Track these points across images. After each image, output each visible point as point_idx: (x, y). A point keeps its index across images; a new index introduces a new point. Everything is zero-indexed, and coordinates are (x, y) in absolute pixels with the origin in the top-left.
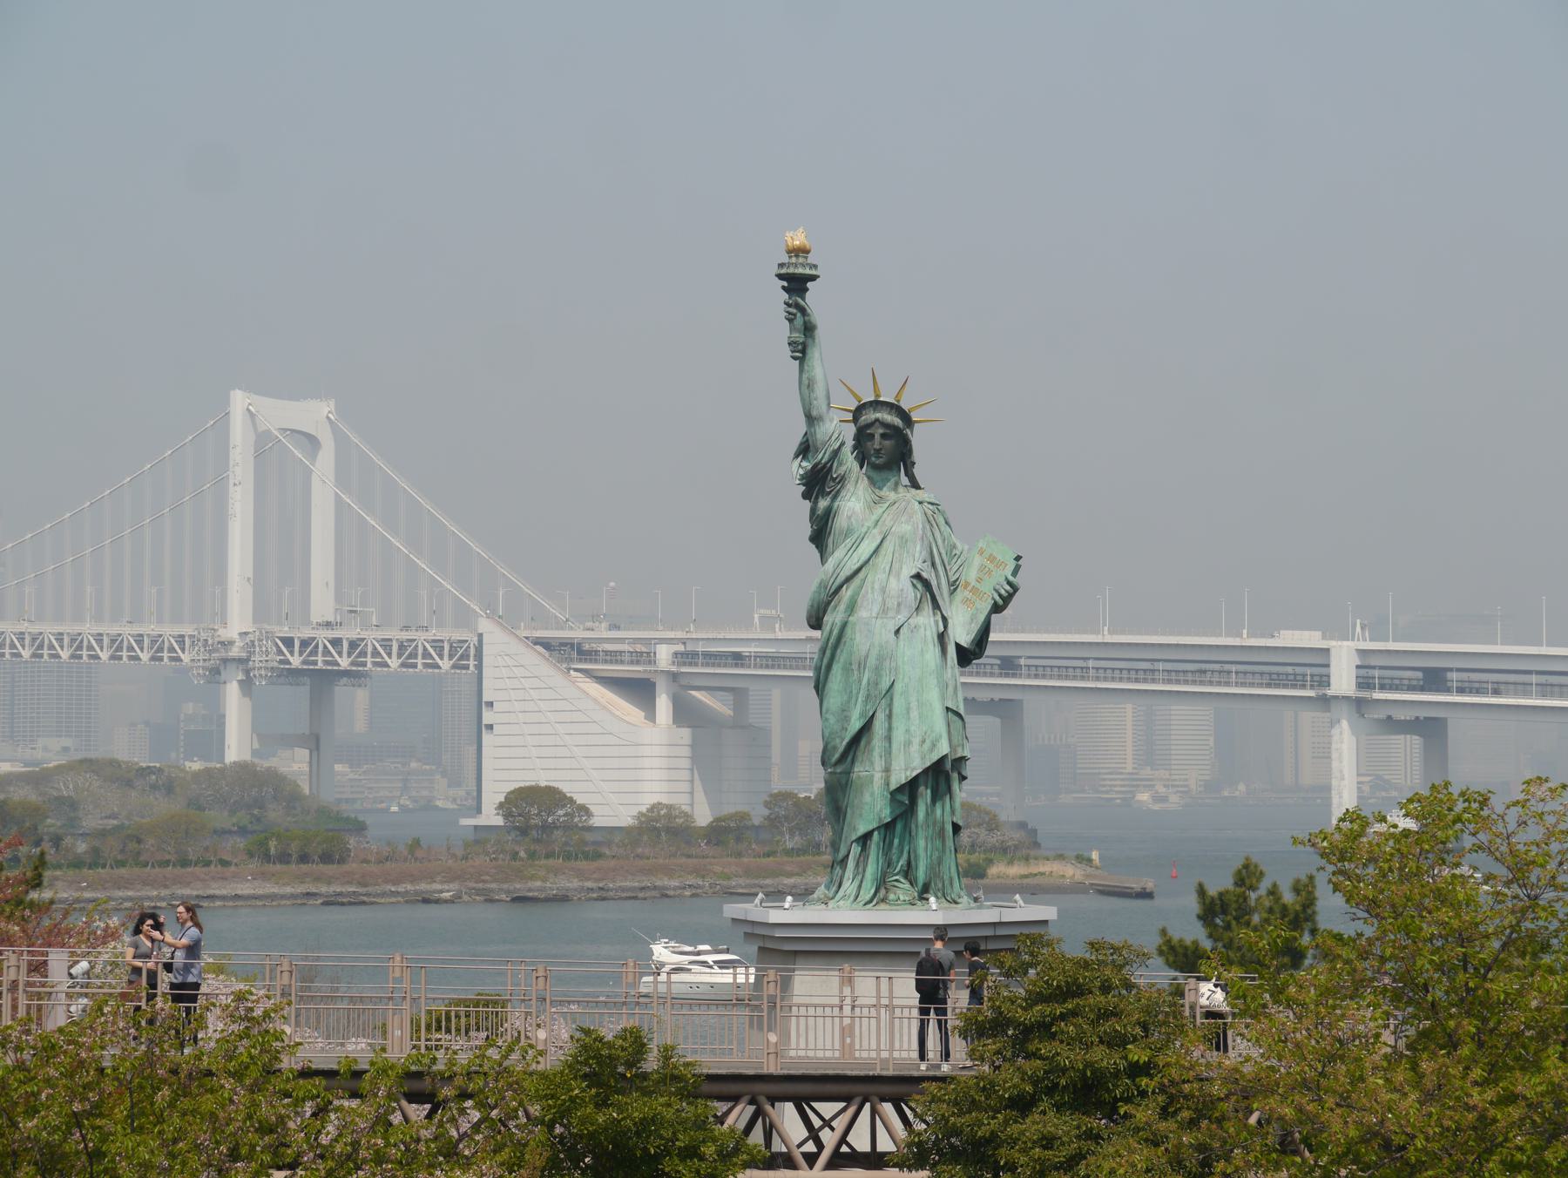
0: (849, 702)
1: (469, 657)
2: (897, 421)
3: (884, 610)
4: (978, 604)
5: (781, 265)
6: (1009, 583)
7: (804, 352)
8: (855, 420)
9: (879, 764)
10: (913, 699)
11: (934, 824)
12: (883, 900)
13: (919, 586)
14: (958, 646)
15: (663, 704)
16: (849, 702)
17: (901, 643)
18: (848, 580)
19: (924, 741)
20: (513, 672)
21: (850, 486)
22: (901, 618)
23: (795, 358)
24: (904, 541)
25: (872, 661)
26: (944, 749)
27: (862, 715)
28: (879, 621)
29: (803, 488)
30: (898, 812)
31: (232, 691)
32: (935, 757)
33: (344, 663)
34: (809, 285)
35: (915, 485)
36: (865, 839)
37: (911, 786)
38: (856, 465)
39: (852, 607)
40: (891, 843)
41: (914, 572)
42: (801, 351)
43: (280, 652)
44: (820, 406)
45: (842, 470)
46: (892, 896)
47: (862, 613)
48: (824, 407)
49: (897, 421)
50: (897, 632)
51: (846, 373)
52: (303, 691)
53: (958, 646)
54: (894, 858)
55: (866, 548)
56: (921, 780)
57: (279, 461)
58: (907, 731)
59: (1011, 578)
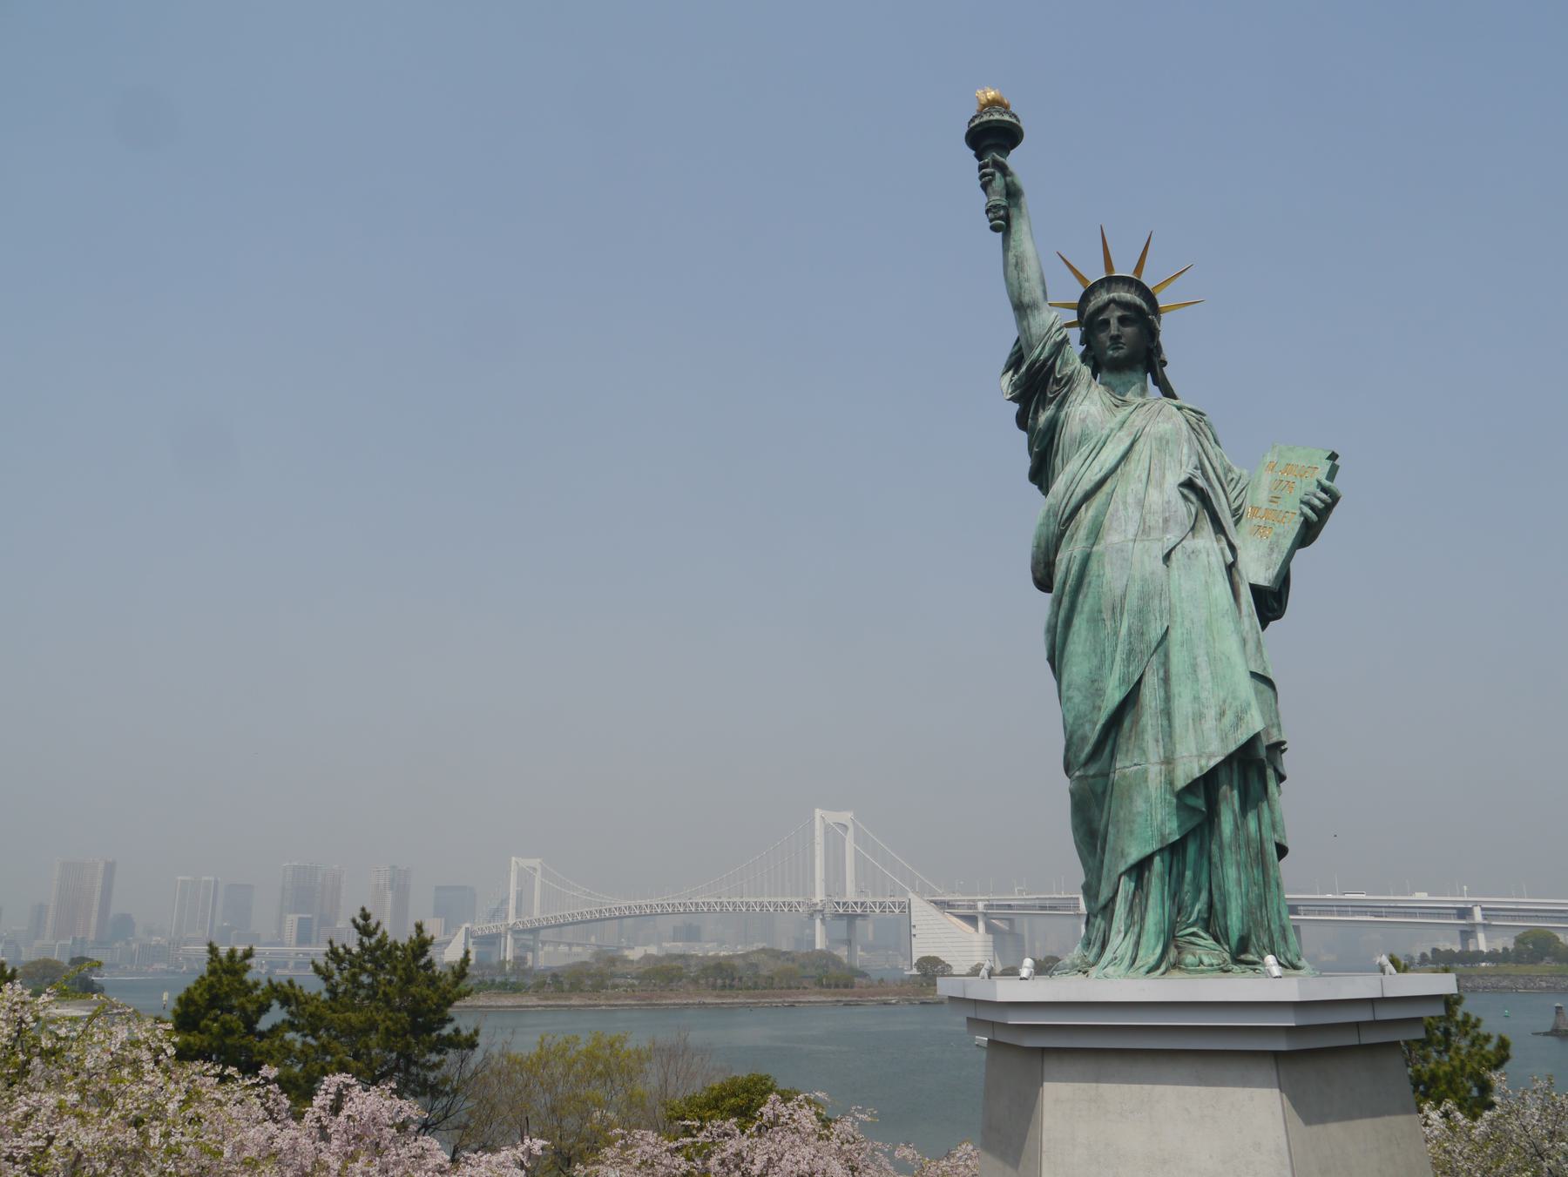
0: (1100, 667)
1: (905, 908)
3: (1145, 531)
4: (1278, 528)
6: (1324, 490)
7: (1007, 219)
9: (1154, 752)
10: (1201, 652)
11: (1248, 845)
12: (1176, 965)
13: (1192, 497)
14: (1255, 589)
15: (981, 925)
16: (1100, 667)
17: (1175, 573)
18: (1088, 496)
19: (1222, 714)
20: (922, 913)
21: (1081, 389)
22: (1171, 538)
23: (995, 229)
24: (1163, 442)
25: (1132, 601)
26: (1255, 723)
27: (1123, 681)
28: (1139, 545)
29: (1016, 407)
30: (1190, 825)
31: (818, 922)
32: (1243, 737)
33: (859, 911)
35: (1168, 392)
36: (1140, 869)
37: (1208, 784)
38: (1086, 371)
39: (1096, 533)
40: (1181, 876)
41: (1183, 478)
42: (1002, 222)
44: (1032, 291)
45: (1068, 370)
46: (1189, 959)
47: (1112, 538)
48: (1039, 294)
50: (1167, 557)
52: (844, 923)
53: (1255, 589)
54: (1188, 898)
56: (1223, 775)
57: (834, 837)
58: (1196, 699)
59: (1327, 483)
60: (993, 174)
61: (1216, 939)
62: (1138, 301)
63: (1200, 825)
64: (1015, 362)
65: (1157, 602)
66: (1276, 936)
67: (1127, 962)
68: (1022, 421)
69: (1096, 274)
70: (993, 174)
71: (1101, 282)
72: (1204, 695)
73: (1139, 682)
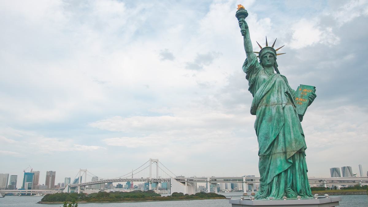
6: (313, 95)
7: (245, 33)
11: (301, 170)
13: (287, 95)
23: (243, 35)
41: (285, 91)
45: (258, 67)
51: (258, 40)
55: (269, 86)
59: (313, 93)
60: (242, 23)
61: (293, 190)
62: (273, 52)
63: (291, 166)
64: (246, 64)
65: (281, 118)
66: (307, 190)
67: (277, 195)
68: (247, 78)
69: (264, 46)
70: (242, 23)
71: (265, 48)
72: (292, 138)
73: (278, 135)
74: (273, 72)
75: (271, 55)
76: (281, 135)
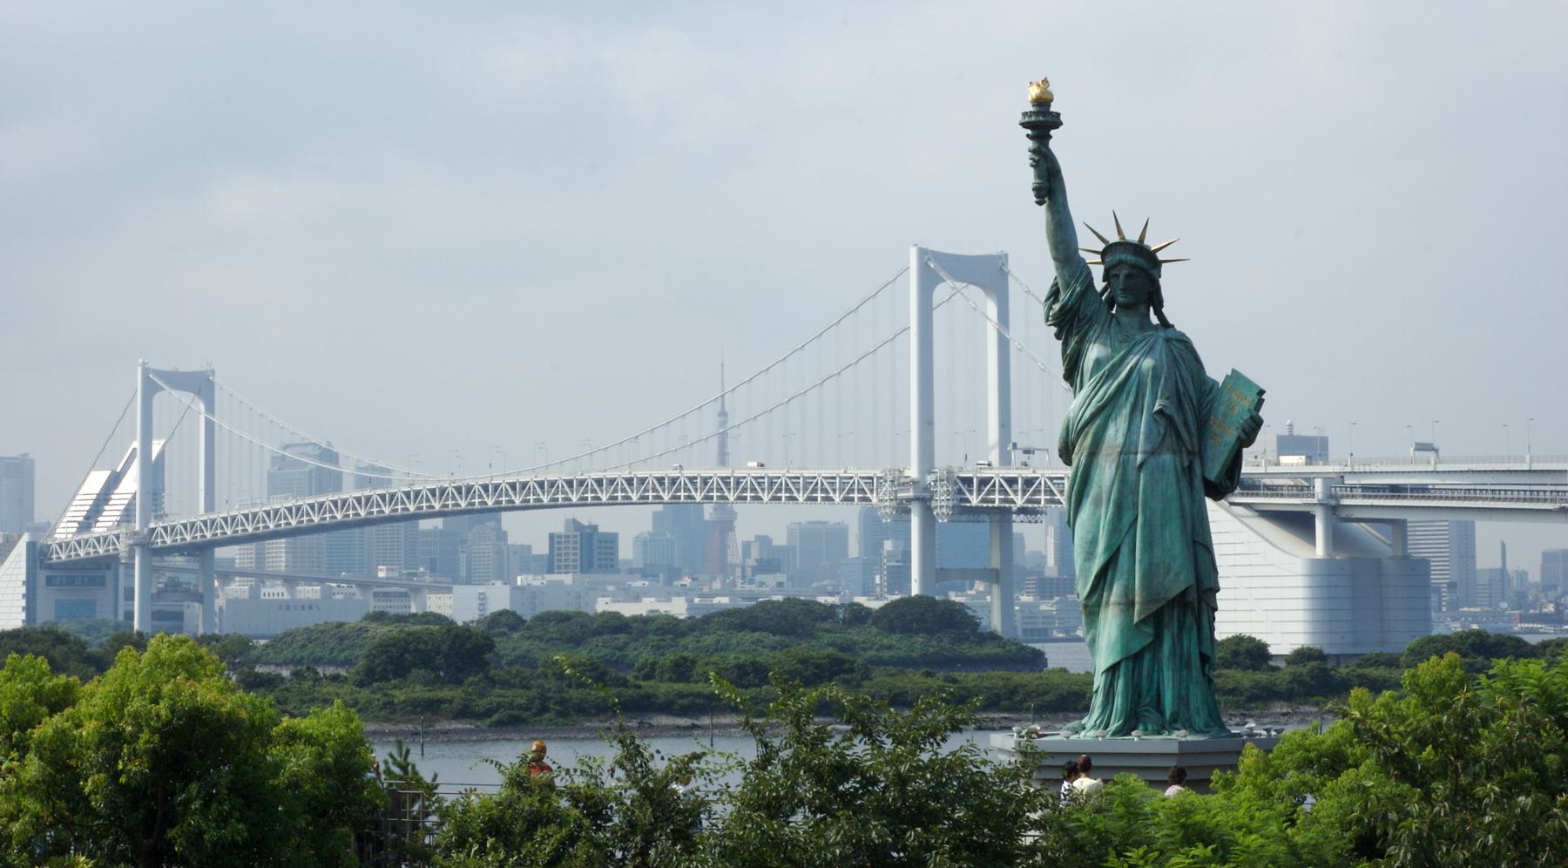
2: (1141, 262)
5: (1025, 114)
8: (1103, 262)
13: (1162, 421)
23: (1040, 203)
34: (1052, 132)
35: (1165, 324)
43: (960, 491)
49: (1141, 262)
64: (1054, 294)
74: (1145, 324)
75: (1134, 272)
76: (1125, 550)
